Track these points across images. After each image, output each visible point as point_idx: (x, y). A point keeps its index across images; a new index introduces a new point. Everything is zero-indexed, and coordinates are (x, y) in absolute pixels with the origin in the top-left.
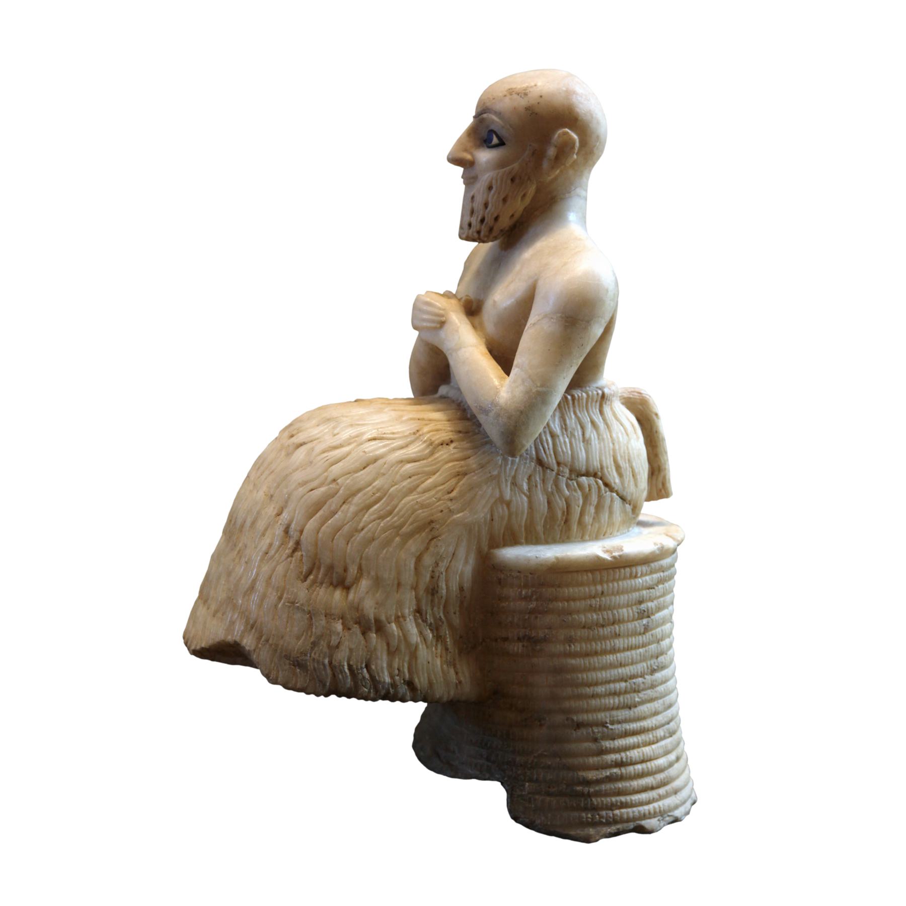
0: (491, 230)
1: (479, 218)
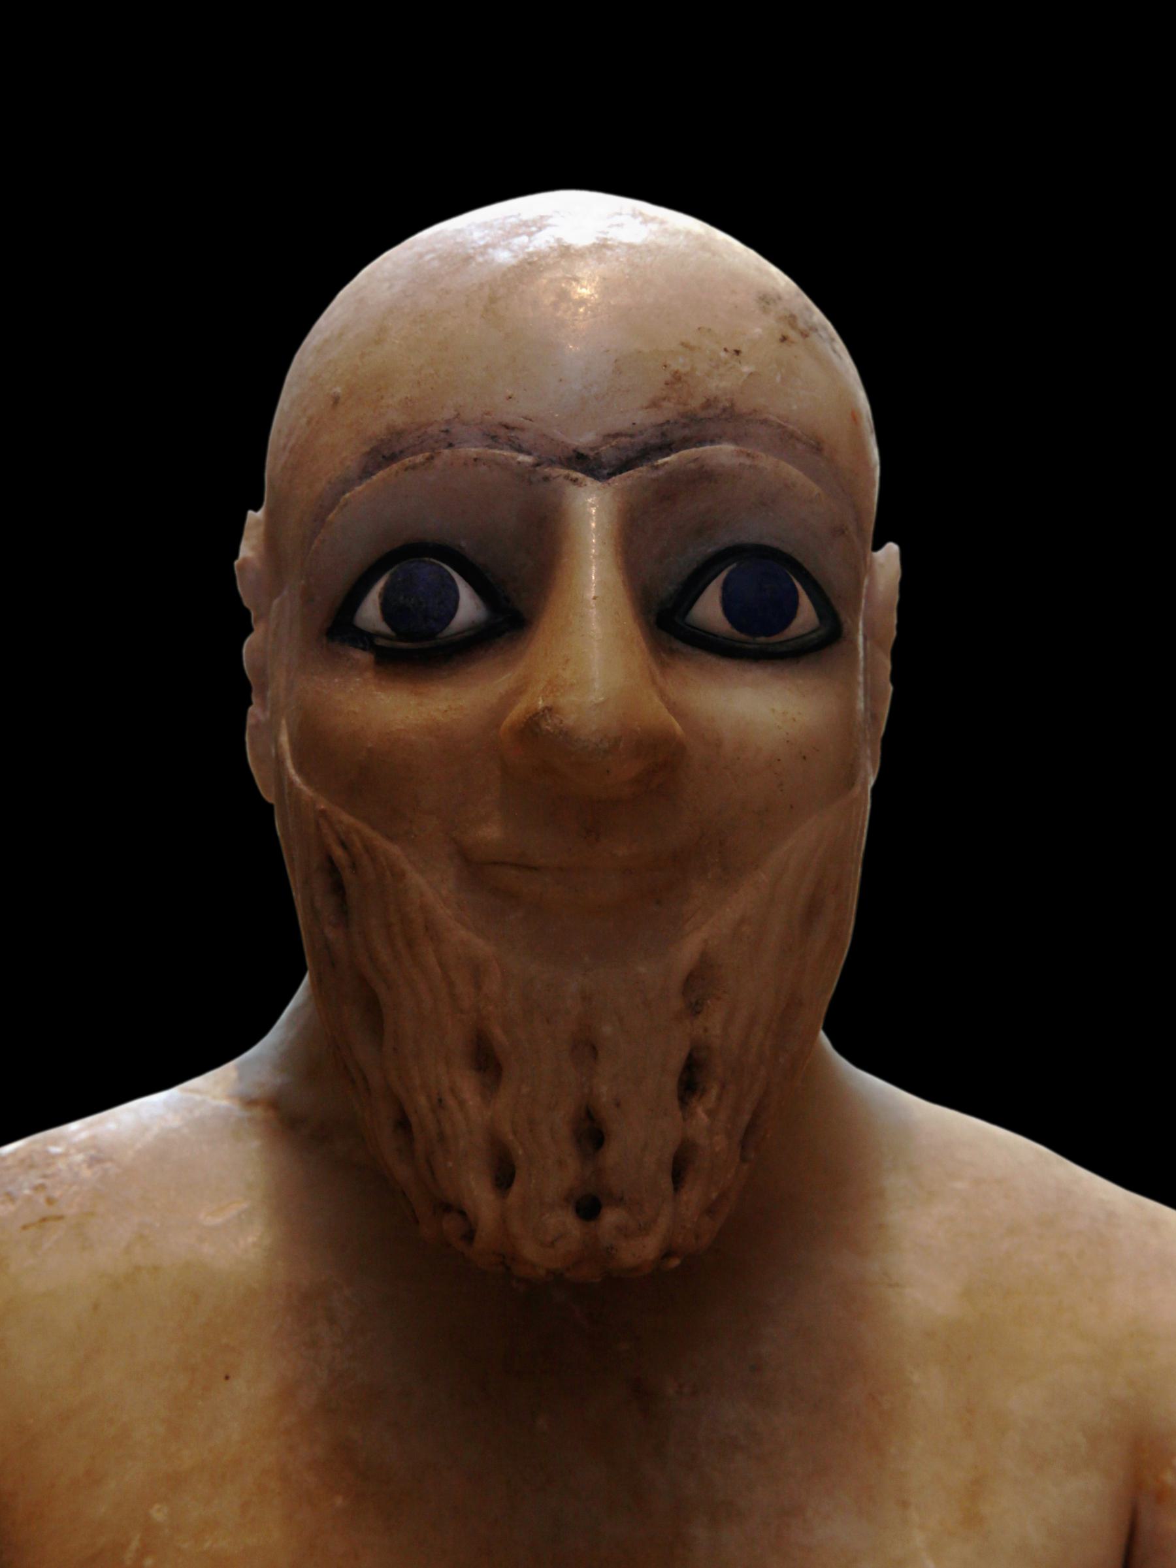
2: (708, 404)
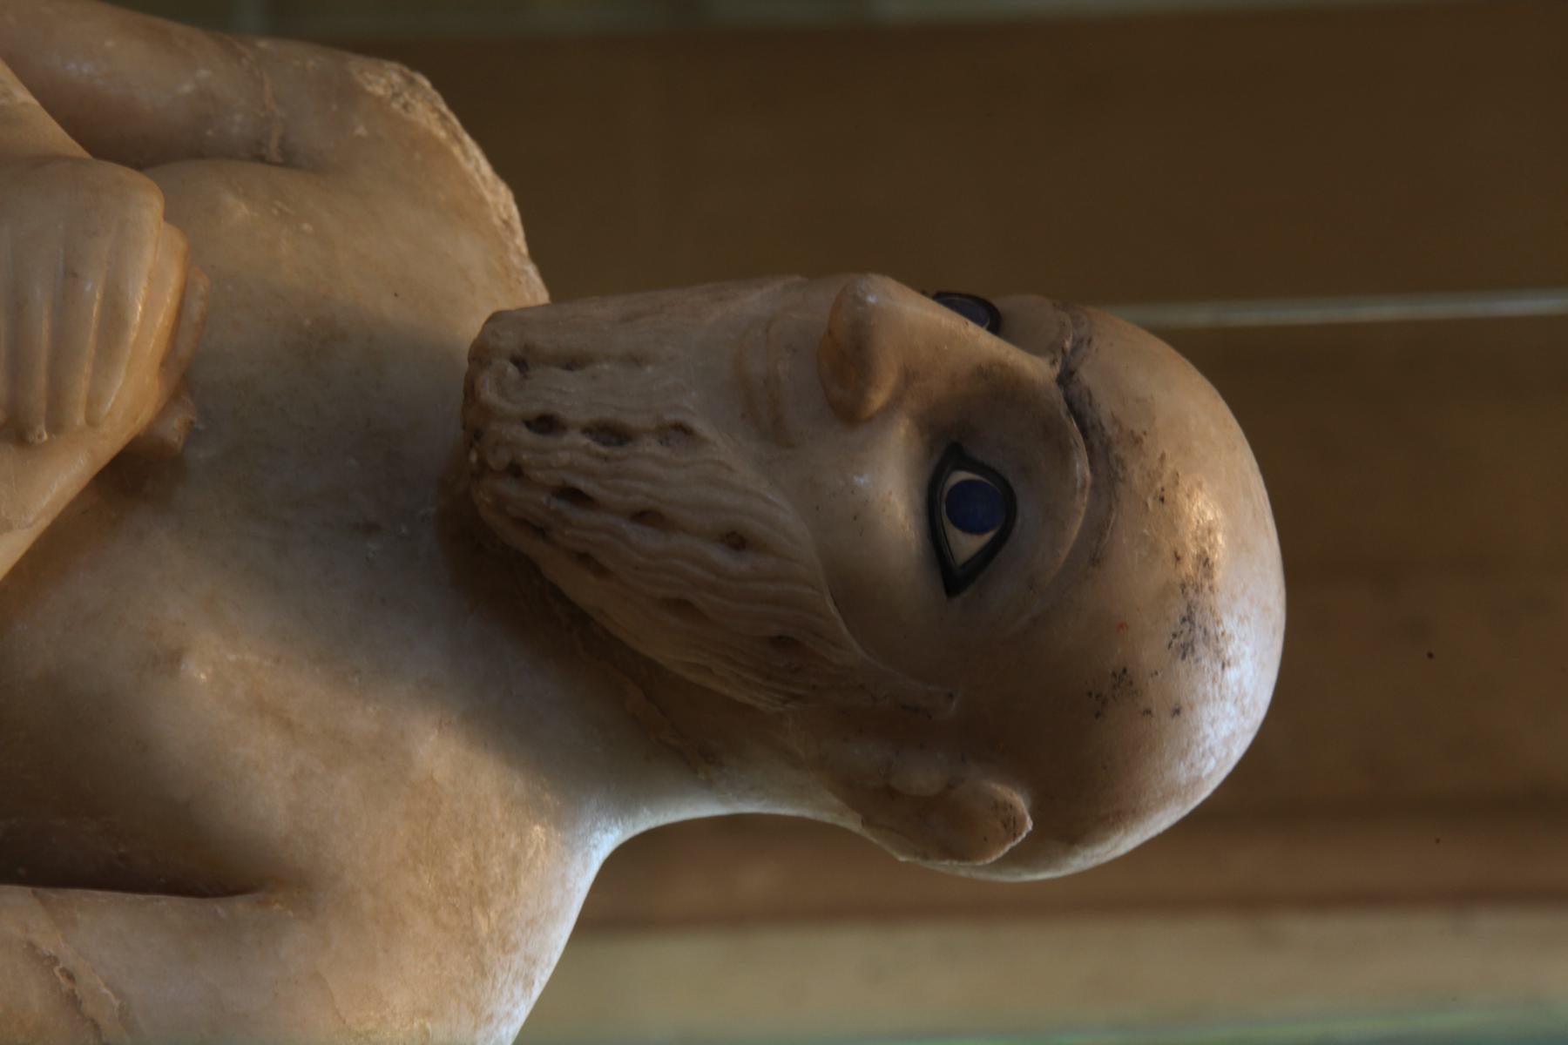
1: (582, 484)
2: (1119, 460)
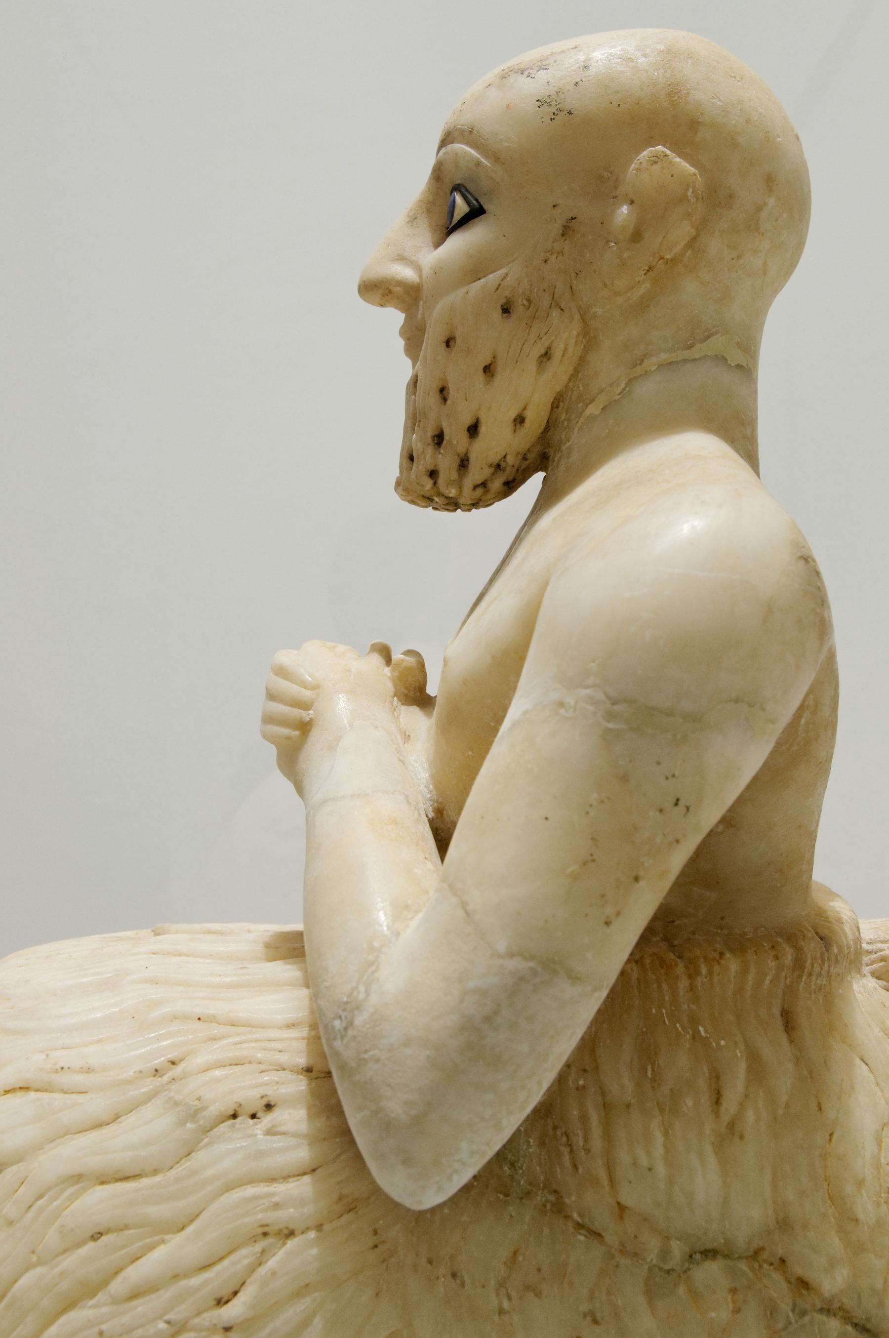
0: (464, 464)
